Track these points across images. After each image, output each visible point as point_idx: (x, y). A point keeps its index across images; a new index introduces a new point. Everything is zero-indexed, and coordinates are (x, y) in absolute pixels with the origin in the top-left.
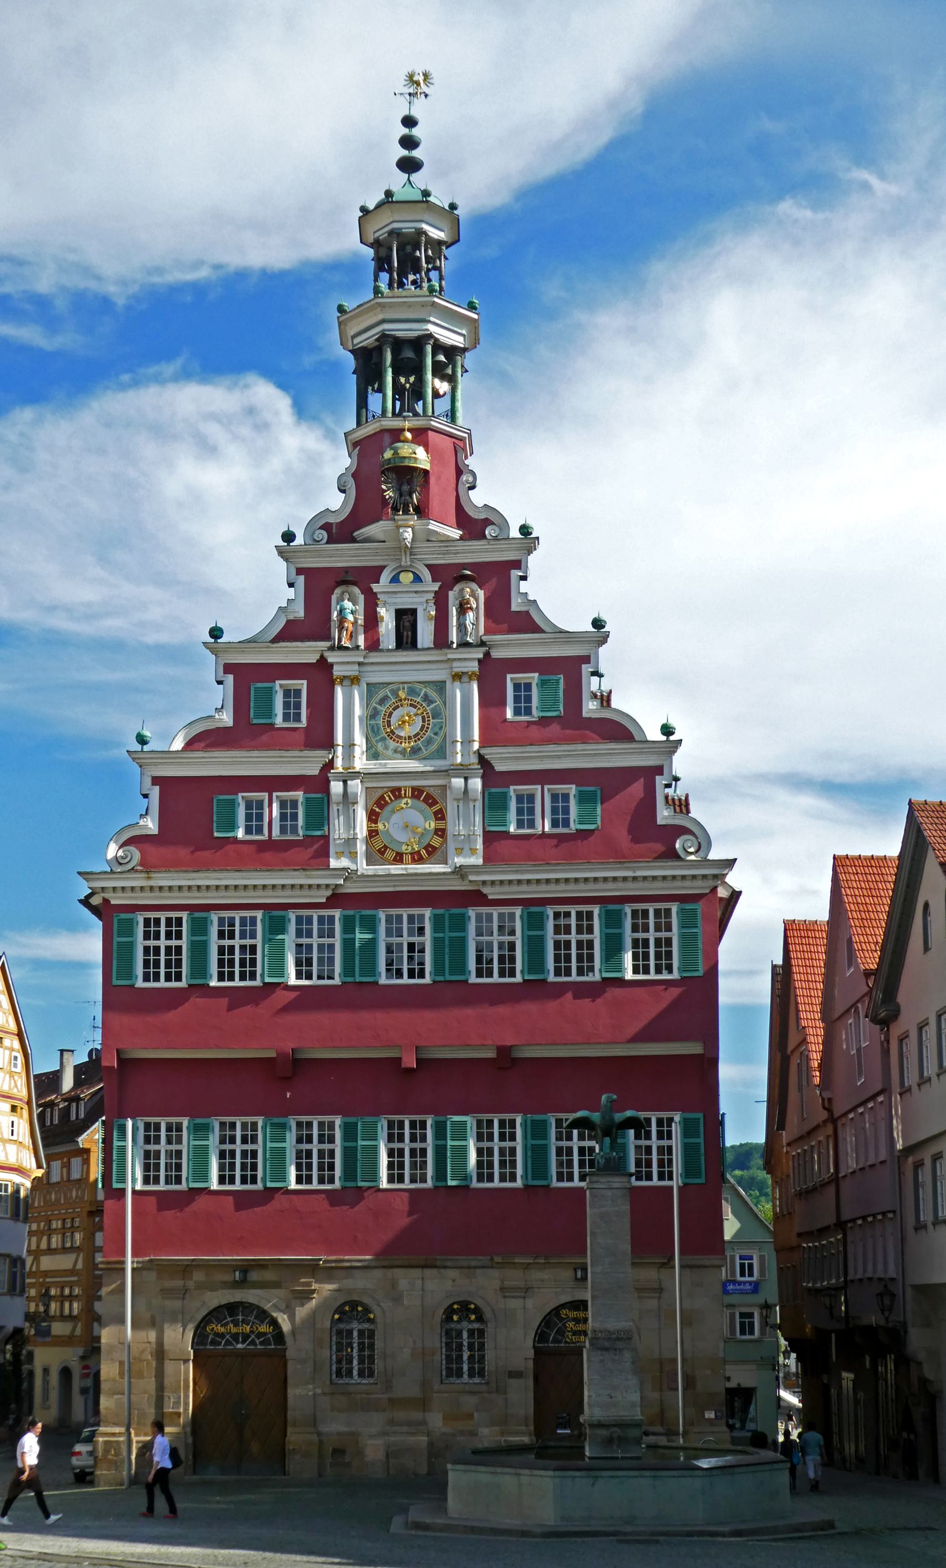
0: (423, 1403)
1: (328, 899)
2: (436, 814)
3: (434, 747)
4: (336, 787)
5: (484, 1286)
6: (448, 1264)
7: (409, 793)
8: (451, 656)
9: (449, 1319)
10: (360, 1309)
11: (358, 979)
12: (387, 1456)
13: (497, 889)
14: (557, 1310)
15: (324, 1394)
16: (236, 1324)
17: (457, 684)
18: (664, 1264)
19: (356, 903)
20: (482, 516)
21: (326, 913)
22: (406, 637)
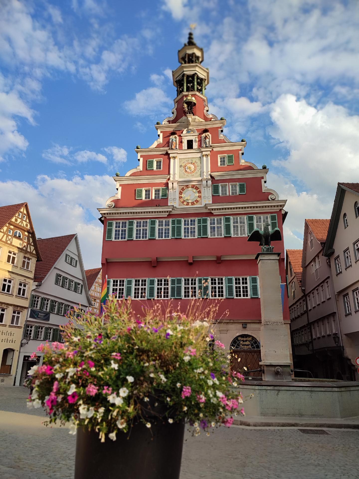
4: (170, 185)
11: (176, 237)
13: (216, 211)
14: (237, 338)
21: (167, 220)
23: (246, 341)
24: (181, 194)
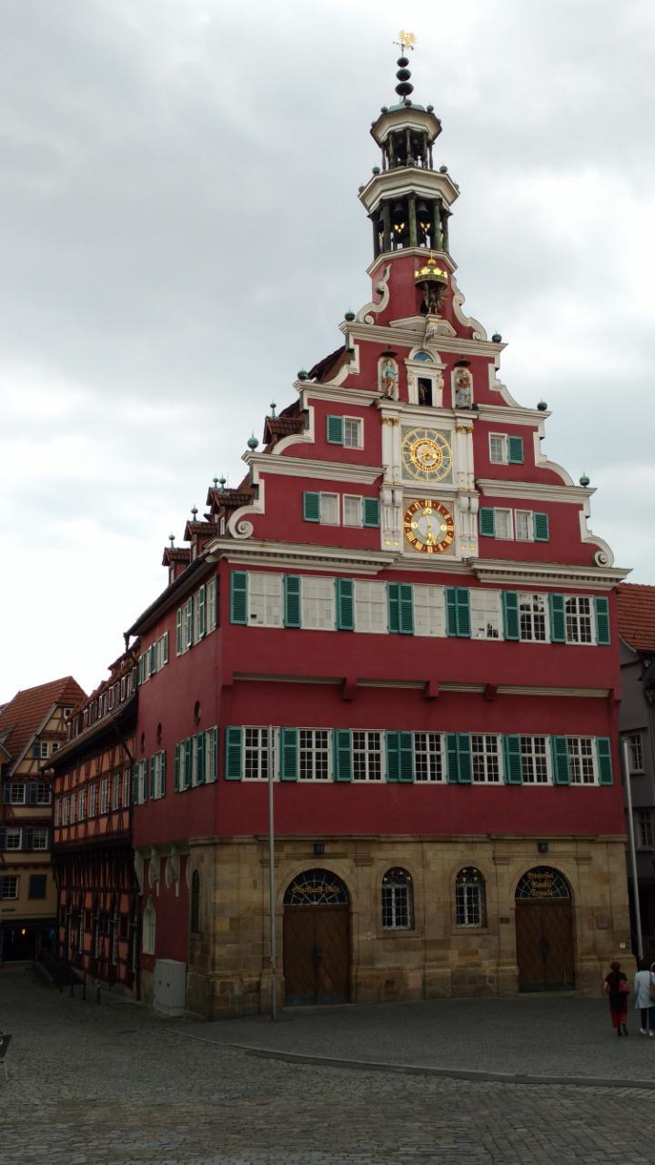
0: (444, 943)
1: (380, 572)
2: (448, 520)
3: (445, 475)
4: (386, 495)
5: (481, 856)
6: (460, 840)
7: (430, 504)
8: (457, 414)
9: (459, 881)
10: (401, 873)
11: (401, 631)
12: (424, 984)
13: (489, 575)
15: (378, 938)
16: (311, 884)
17: (459, 434)
18: (593, 840)
19: (400, 579)
20: (469, 325)
22: (426, 400)
23: (543, 881)
24: (409, 522)
